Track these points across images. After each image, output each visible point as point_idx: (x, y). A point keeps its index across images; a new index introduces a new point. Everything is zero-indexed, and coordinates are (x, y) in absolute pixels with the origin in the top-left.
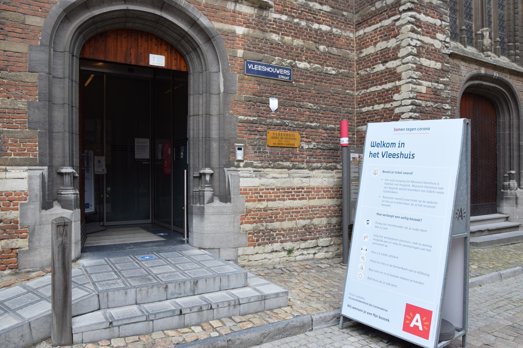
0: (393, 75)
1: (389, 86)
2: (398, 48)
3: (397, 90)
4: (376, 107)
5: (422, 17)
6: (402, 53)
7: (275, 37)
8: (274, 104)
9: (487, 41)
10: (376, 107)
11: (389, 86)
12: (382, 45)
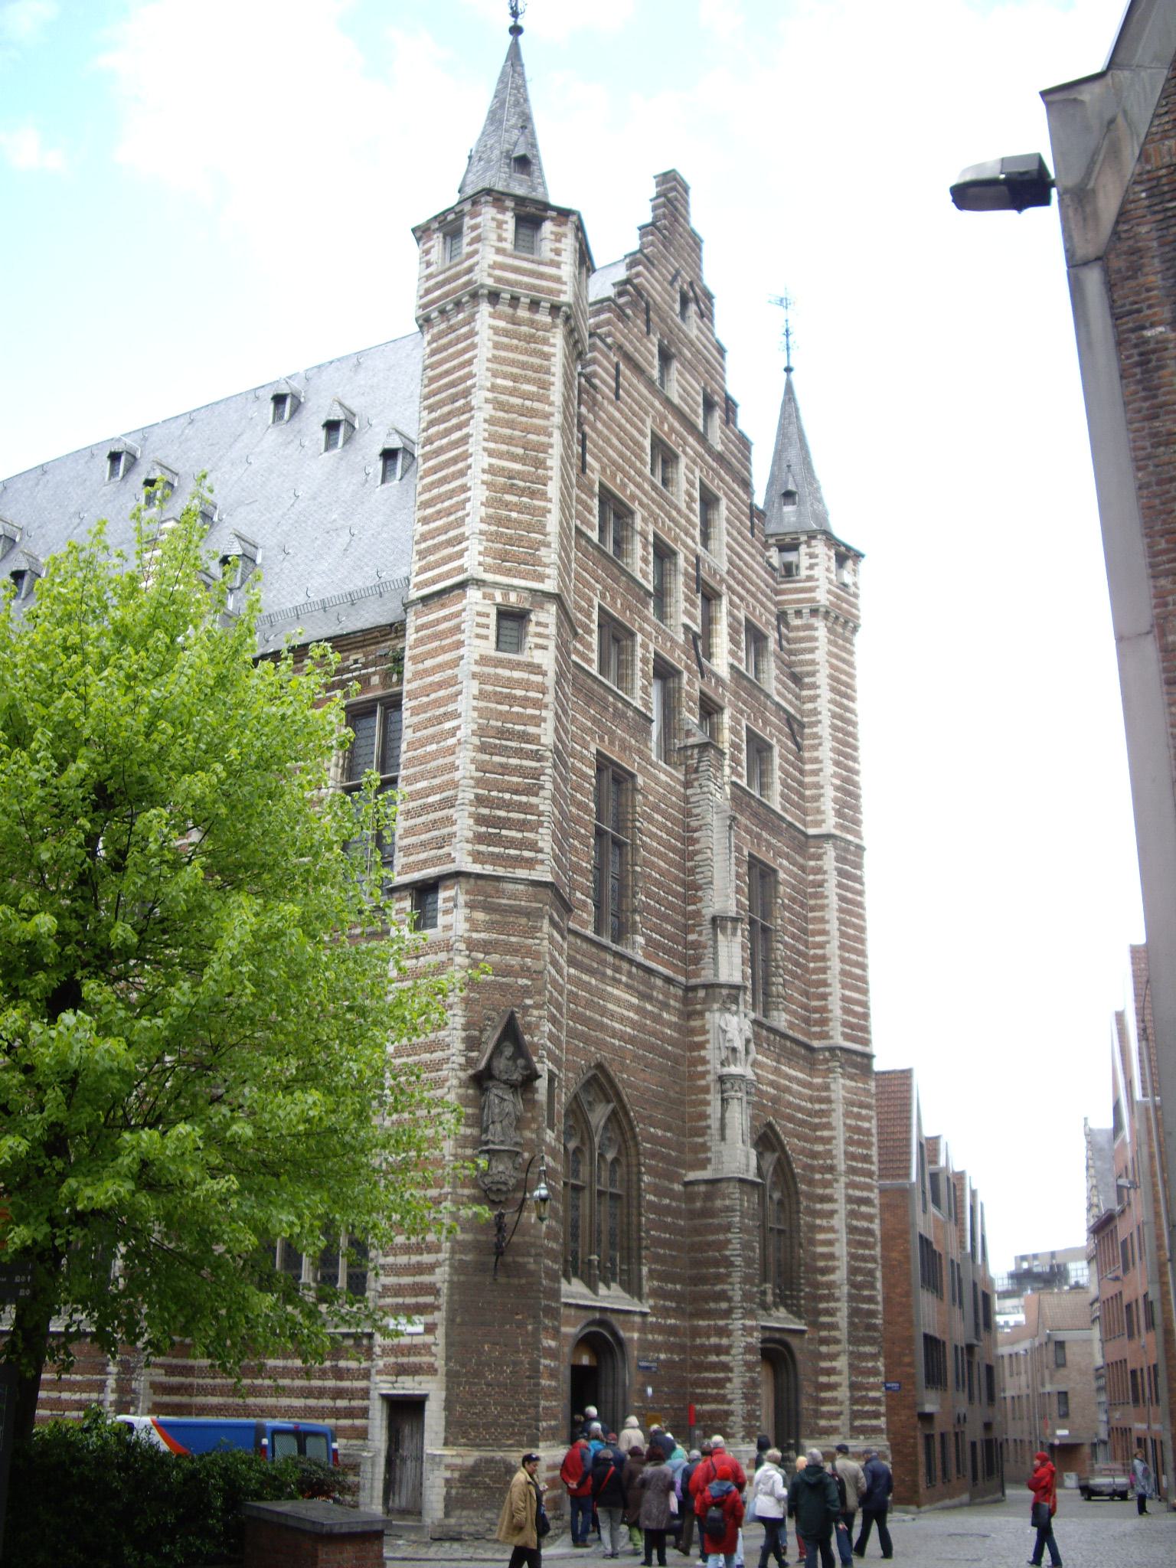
0: (726, 1367)
1: (721, 1375)
2: (730, 1347)
3: (729, 1380)
4: (710, 1391)
5: (749, 1323)
6: (734, 1351)
7: (650, 1337)
8: (650, 1390)
9: (770, 1298)
10: (710, 1391)
11: (721, 1375)
12: (714, 1340)
